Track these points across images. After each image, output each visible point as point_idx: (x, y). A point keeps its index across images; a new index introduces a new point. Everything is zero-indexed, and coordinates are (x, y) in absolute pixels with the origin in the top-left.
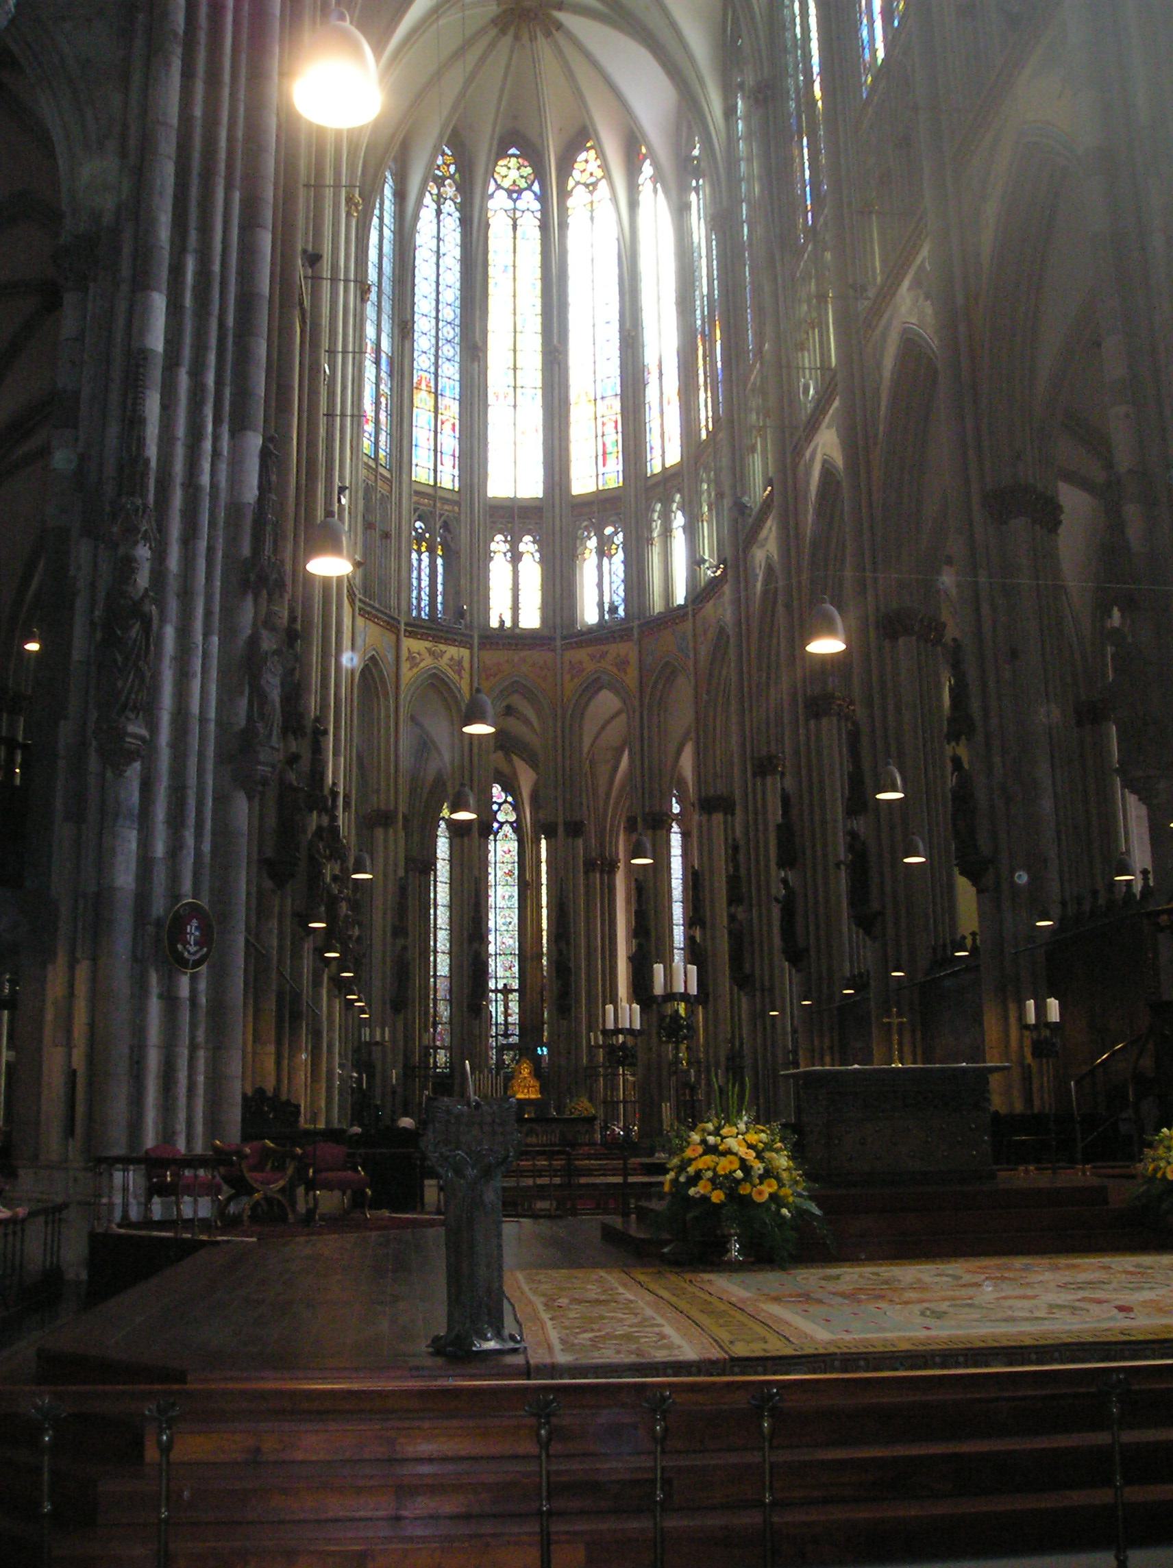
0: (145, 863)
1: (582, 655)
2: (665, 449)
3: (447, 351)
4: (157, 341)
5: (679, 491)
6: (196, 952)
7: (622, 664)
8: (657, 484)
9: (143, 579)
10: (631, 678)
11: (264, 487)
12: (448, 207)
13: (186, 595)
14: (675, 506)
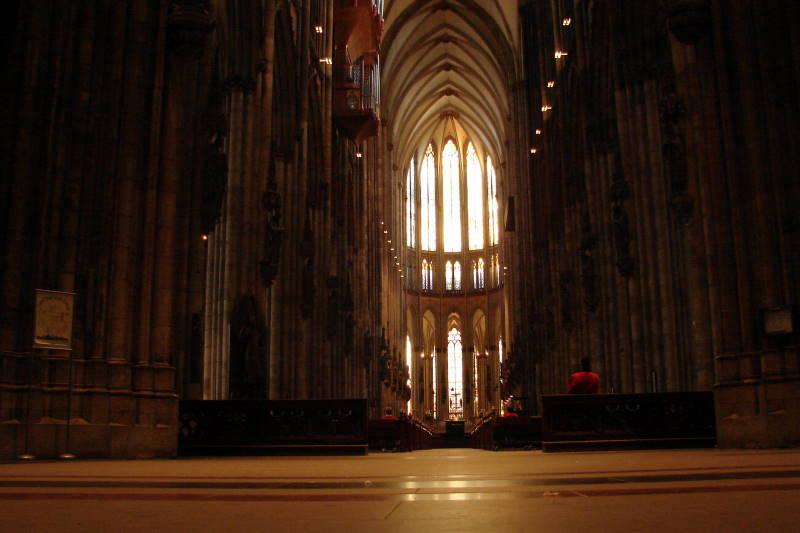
7: (483, 302)
10: (486, 306)
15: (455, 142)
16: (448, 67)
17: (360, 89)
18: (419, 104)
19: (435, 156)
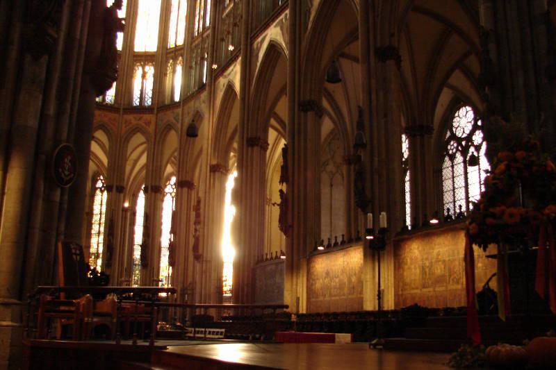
0: (43, 117)
1: (130, 117)
2: (177, 37)
5: (182, 56)
6: (69, 175)
7: (148, 123)
8: (172, 52)
10: (151, 129)
14: (178, 62)
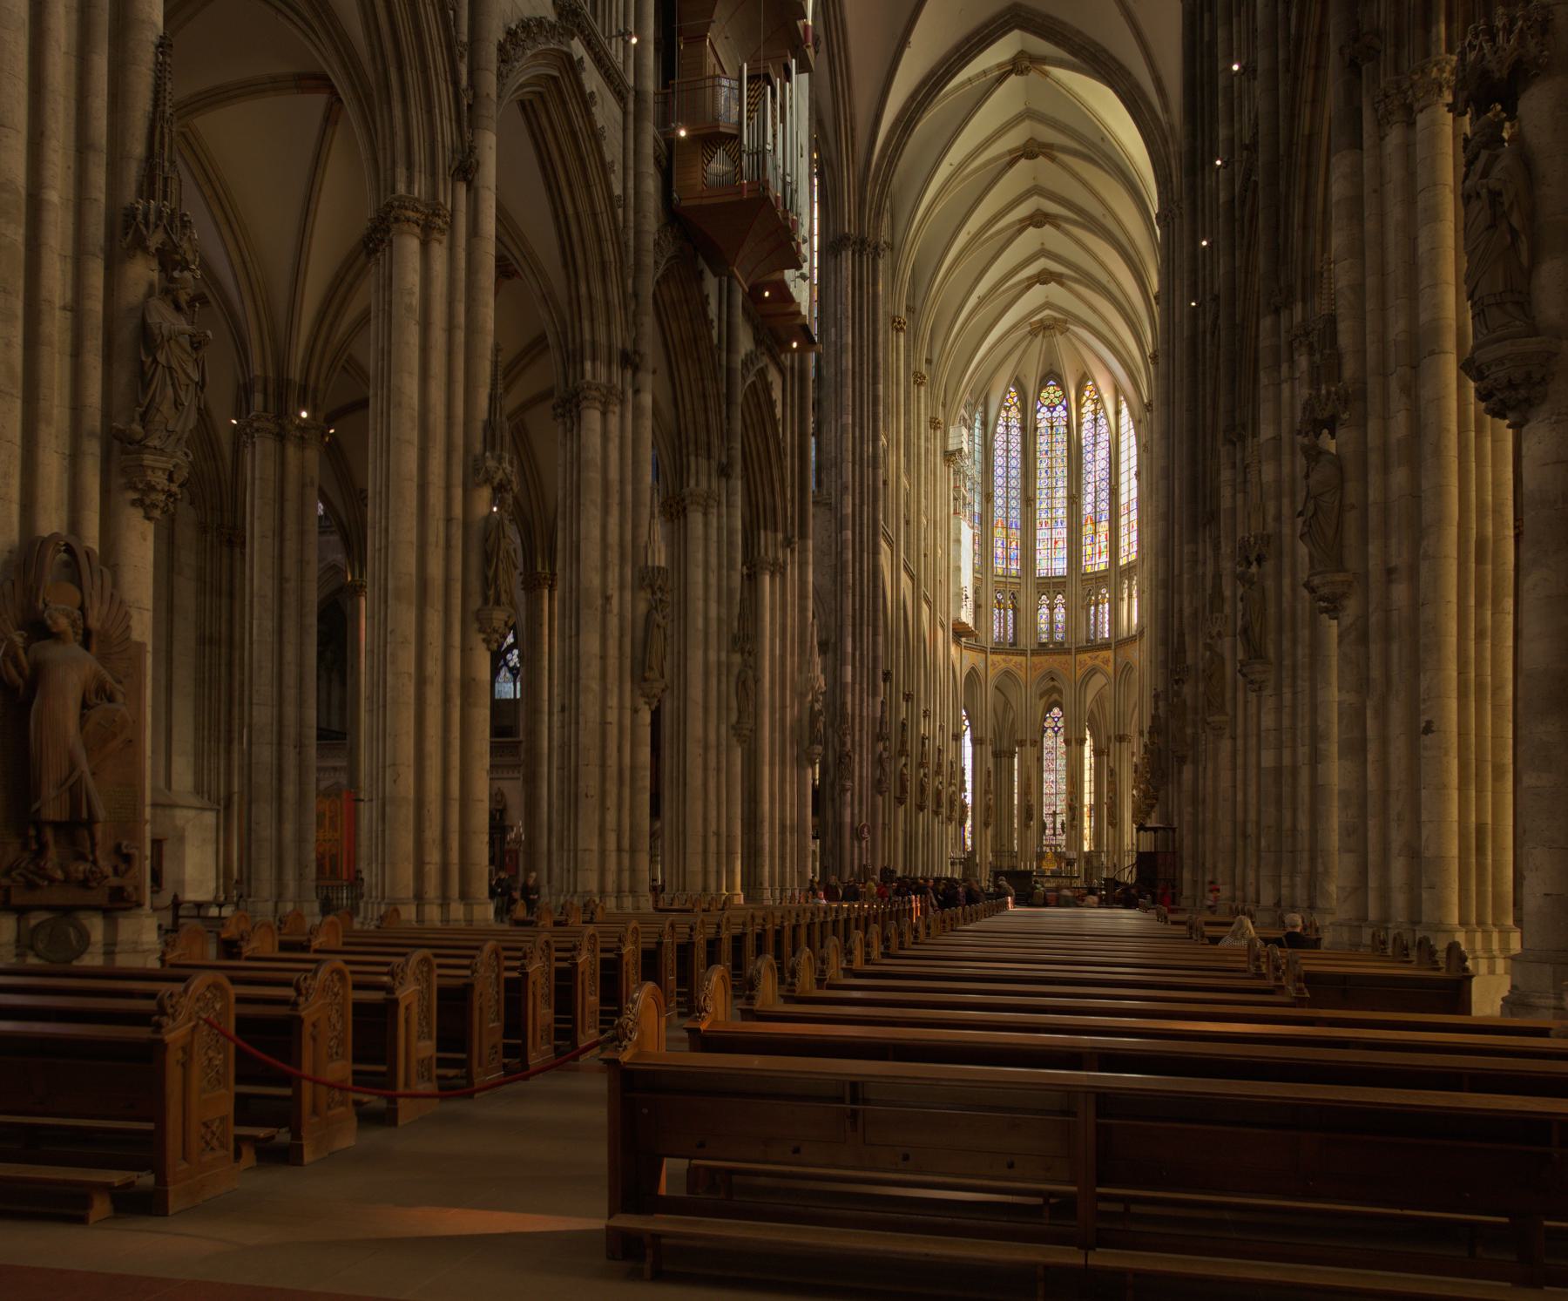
1: (1084, 657)
3: (1013, 503)
4: (849, 679)
7: (1107, 662)
9: (849, 745)
10: (1110, 669)
11: (883, 712)
12: (1014, 422)
13: (861, 746)
15: (1061, 385)
16: (1038, 219)
17: (732, 139)
18: (982, 301)
19: (1023, 410)
